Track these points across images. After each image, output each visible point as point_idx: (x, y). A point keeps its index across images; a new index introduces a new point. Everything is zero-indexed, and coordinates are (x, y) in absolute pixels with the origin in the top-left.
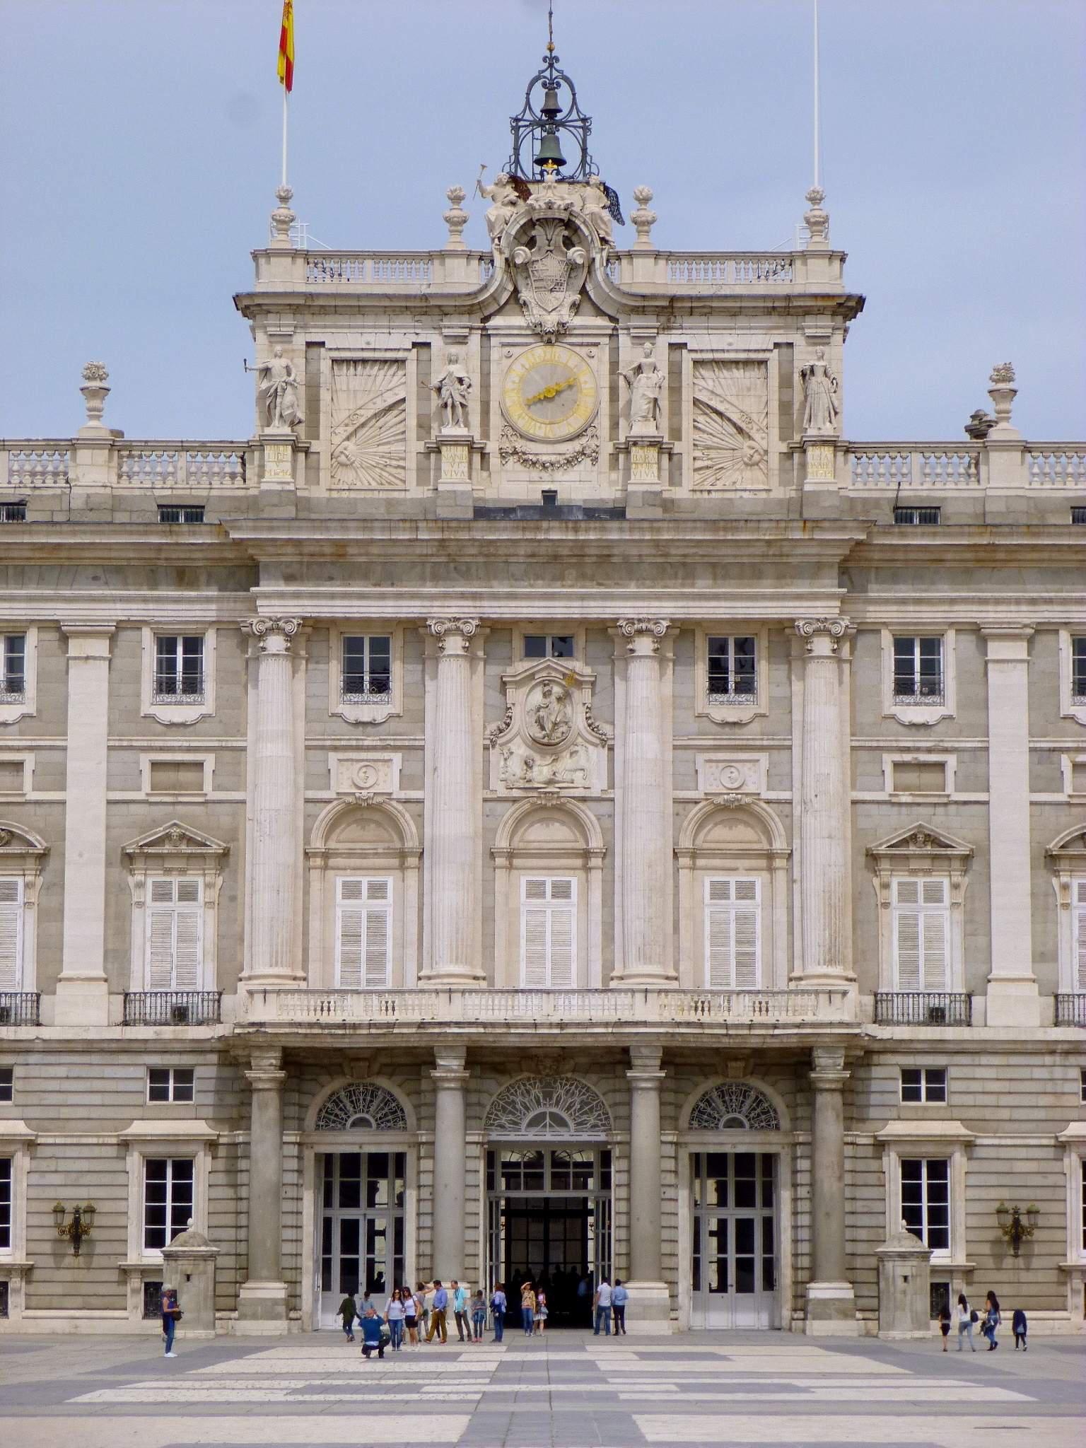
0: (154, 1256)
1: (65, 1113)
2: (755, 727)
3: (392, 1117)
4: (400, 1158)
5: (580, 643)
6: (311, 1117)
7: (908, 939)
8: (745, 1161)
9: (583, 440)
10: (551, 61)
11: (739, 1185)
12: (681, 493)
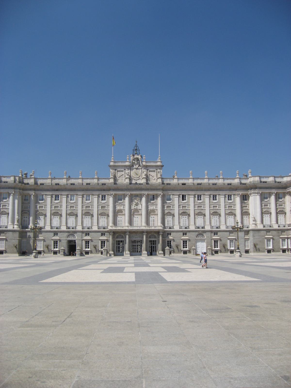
0: (102, 249)
1: (94, 237)
2: (154, 203)
3: (123, 237)
4: (123, 241)
5: (139, 195)
6: (115, 238)
7: (168, 222)
8: (153, 241)
9: (139, 178)
10: (136, 145)
11: (153, 243)
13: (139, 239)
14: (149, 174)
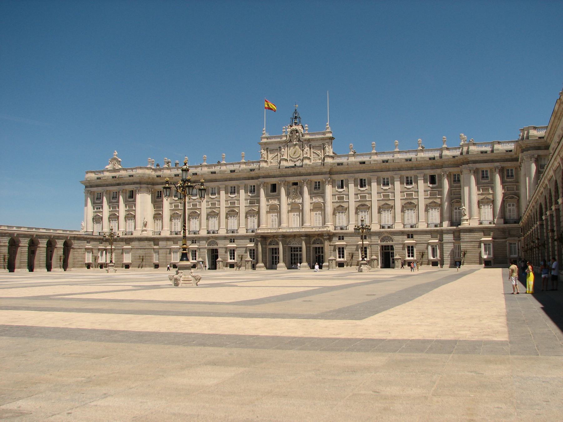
1: (240, 244)
7: (339, 219)
8: (319, 248)
9: (299, 158)
10: (296, 110)
12: (311, 163)
13: (298, 246)
14: (313, 152)
